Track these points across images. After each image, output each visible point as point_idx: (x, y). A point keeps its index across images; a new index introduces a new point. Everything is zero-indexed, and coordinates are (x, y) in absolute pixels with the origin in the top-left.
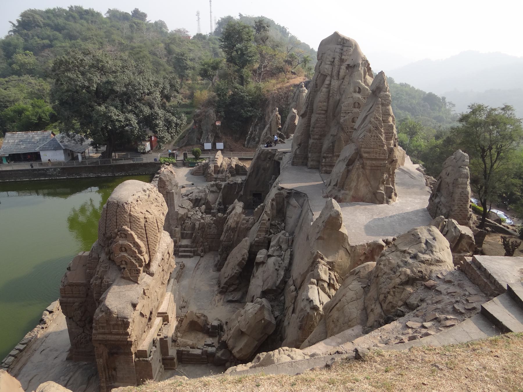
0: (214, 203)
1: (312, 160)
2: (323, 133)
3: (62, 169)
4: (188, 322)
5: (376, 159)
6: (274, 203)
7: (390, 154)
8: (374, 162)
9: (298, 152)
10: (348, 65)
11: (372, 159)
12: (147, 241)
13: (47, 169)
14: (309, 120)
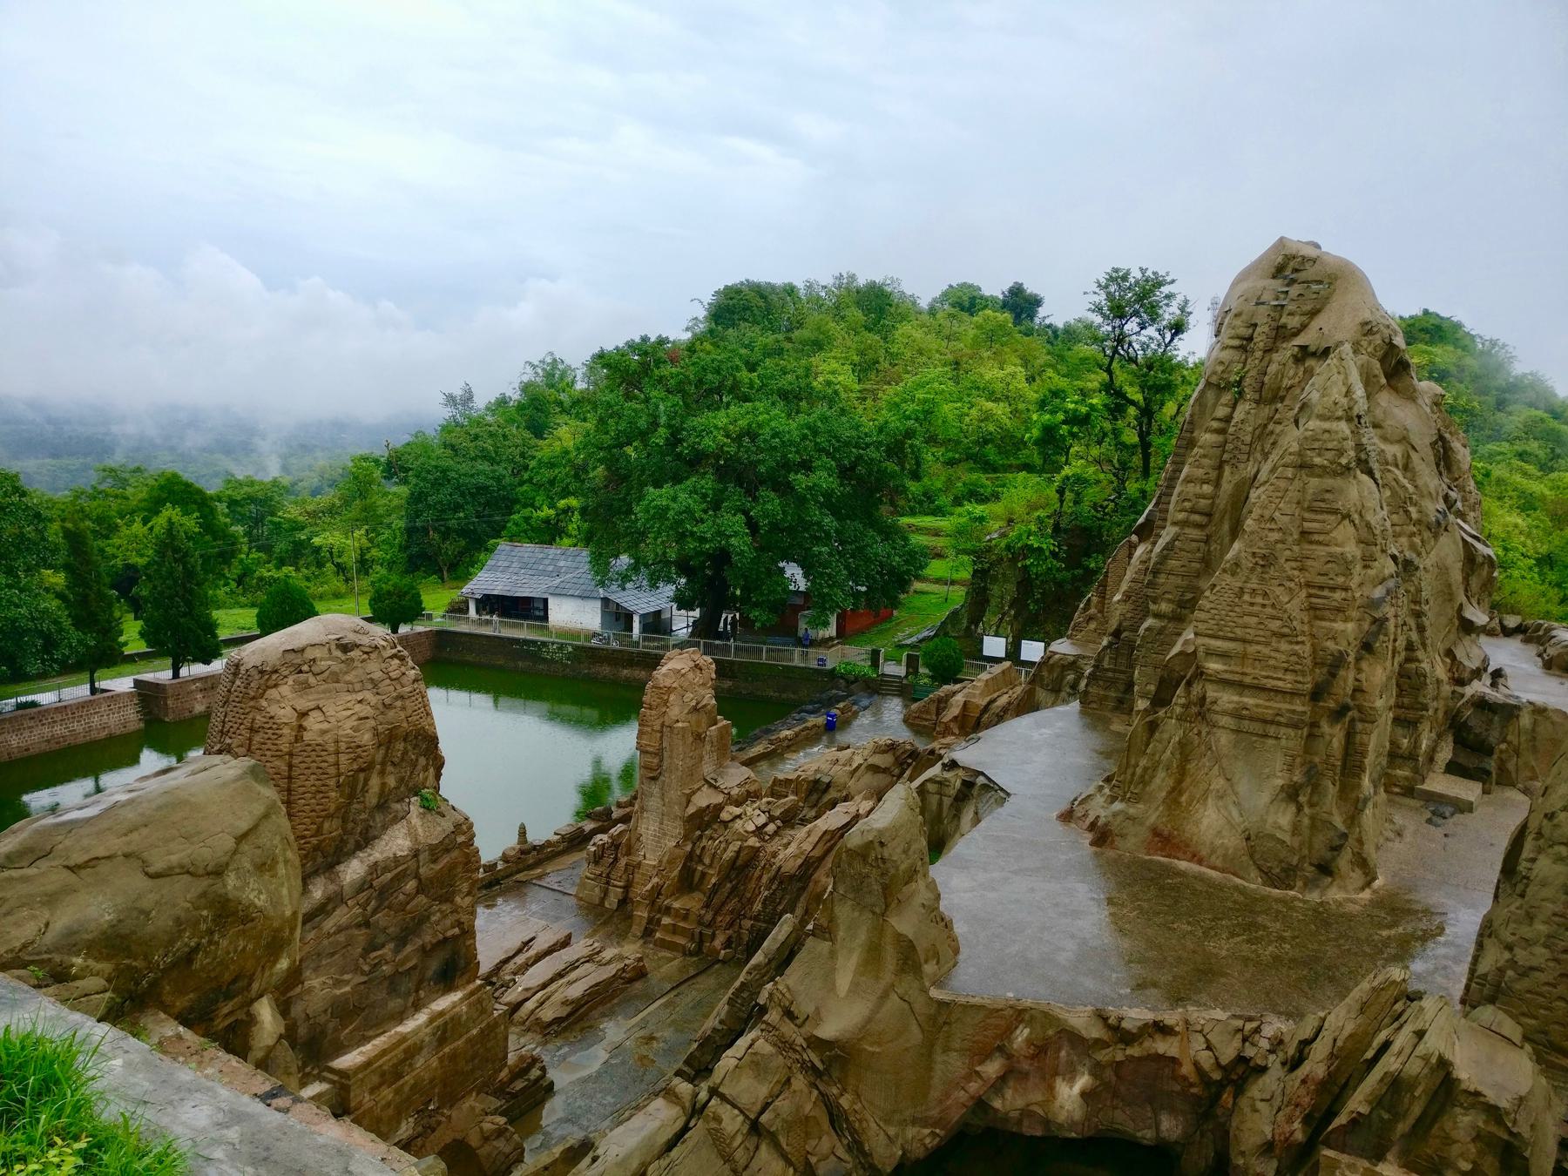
2: (1189, 596)
3: (576, 648)
4: (448, 1140)
5: (1259, 689)
7: (1334, 675)
8: (1249, 701)
10: (1303, 348)
11: (1240, 687)
13: (544, 644)
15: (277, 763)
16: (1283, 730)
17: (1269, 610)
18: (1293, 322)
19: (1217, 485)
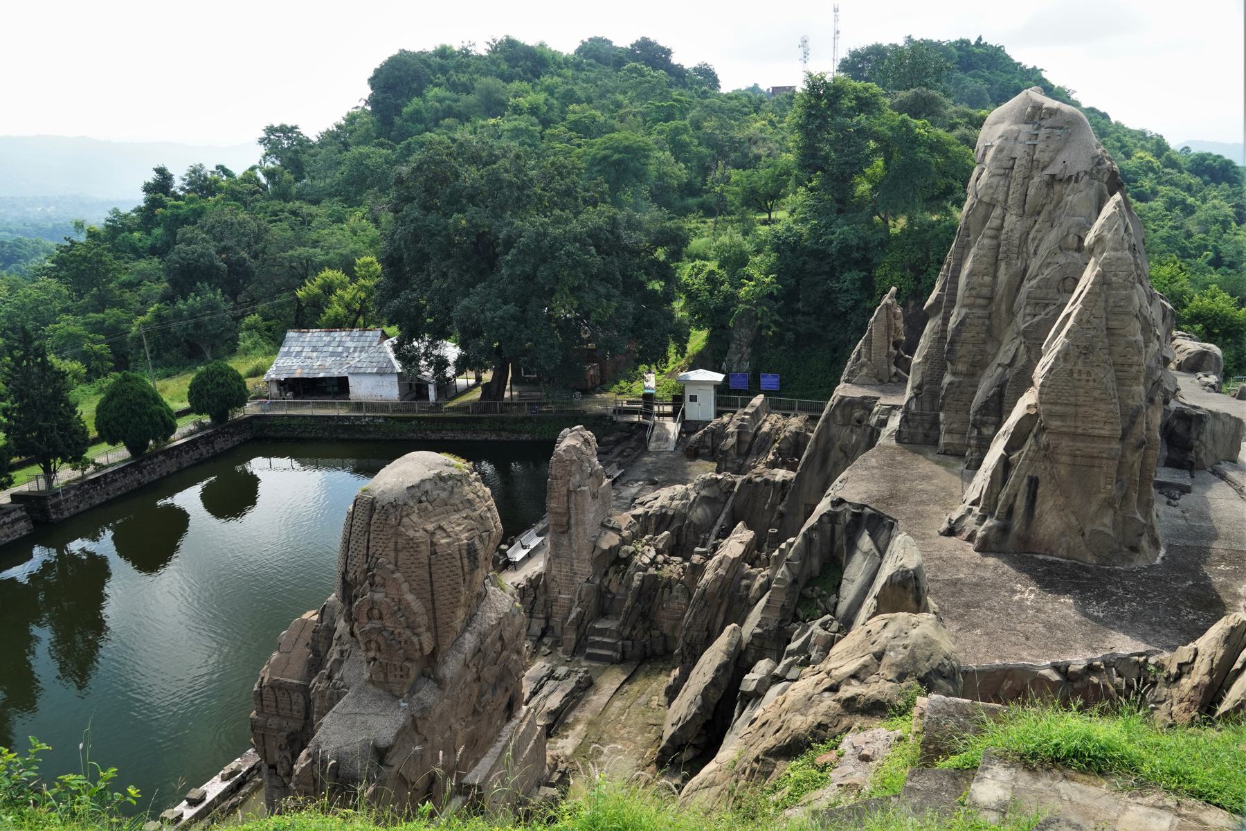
0: (709, 531)
1: (949, 432)
6: (815, 536)
8: (1080, 445)
9: (913, 407)
10: (1053, 176)
11: (1074, 436)
12: (433, 600)
14: (946, 321)
15: (419, 572)
16: (1104, 462)
17: (1091, 383)
18: (1045, 157)
19: (995, 277)
